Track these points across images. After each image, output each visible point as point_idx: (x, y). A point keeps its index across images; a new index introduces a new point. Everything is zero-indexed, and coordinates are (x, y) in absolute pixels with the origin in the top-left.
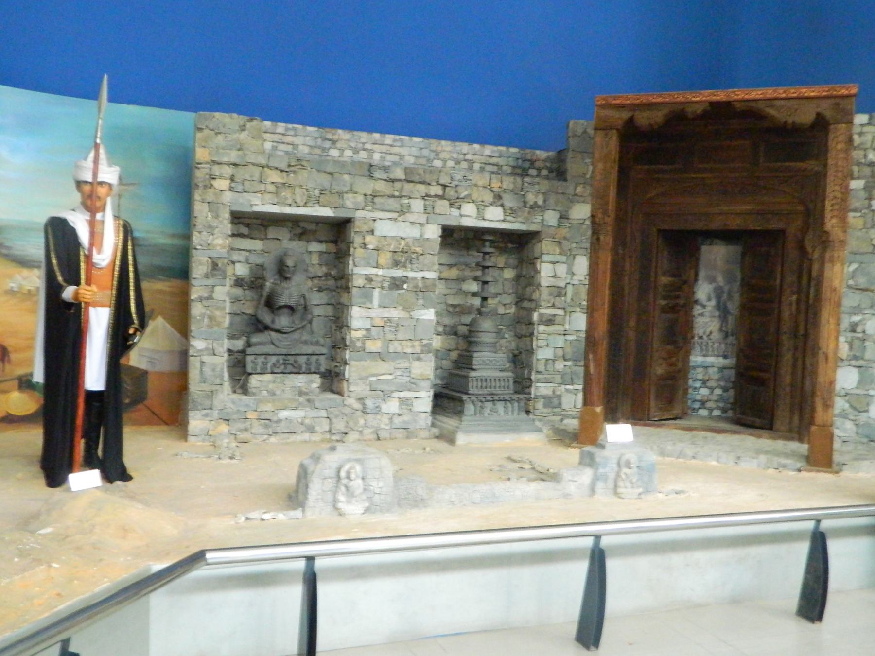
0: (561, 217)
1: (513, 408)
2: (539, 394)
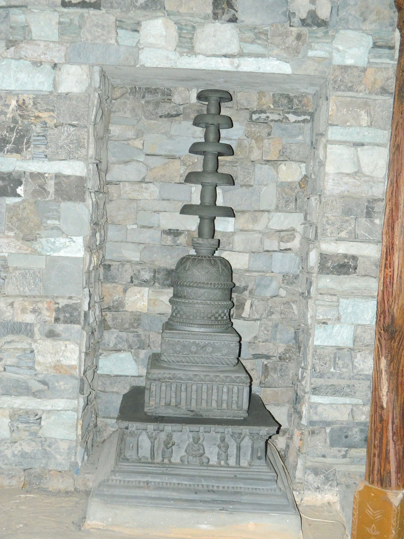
0: (375, 46)
1: (239, 448)
2: (315, 418)
